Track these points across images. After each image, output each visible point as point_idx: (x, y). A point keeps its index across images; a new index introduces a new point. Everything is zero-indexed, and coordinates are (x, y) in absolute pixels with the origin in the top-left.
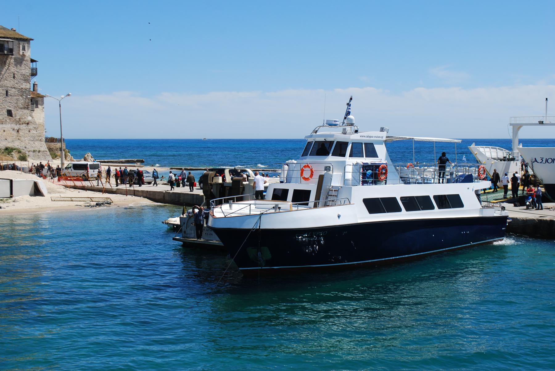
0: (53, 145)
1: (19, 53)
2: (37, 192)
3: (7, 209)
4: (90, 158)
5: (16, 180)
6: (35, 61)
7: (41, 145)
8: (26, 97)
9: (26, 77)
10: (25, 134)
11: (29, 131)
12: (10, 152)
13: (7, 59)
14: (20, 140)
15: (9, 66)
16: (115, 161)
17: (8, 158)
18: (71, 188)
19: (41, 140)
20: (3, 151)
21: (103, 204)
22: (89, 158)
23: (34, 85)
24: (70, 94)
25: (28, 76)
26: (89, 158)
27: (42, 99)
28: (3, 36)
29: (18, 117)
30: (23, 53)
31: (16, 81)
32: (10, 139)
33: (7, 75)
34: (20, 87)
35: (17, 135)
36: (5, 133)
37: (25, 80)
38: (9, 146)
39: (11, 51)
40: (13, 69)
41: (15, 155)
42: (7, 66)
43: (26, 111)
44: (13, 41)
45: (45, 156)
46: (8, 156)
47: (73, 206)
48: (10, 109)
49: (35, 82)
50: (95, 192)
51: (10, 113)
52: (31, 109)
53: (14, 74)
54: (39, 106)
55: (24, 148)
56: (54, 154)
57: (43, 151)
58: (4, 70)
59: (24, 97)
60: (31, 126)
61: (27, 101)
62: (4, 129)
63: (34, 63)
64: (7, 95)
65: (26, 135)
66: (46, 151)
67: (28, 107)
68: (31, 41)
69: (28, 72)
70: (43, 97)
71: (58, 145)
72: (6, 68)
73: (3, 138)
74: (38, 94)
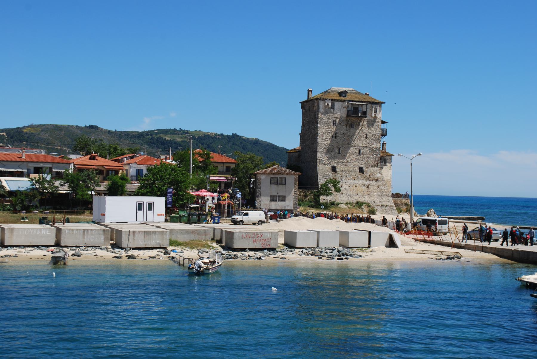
0: (398, 200)
1: (371, 115)
2: (392, 243)
3: (366, 258)
4: (433, 214)
5: (374, 232)
6: (386, 123)
7: (388, 201)
8: (377, 155)
9: (376, 137)
10: (374, 190)
11: (378, 187)
12: (361, 206)
13: (360, 121)
14: (370, 195)
15: (362, 127)
16: (456, 218)
17: (359, 211)
18: (421, 241)
19: (388, 196)
20: (354, 204)
21: (453, 258)
22: (432, 214)
23: (383, 144)
24: (421, 153)
25: (378, 136)
26: (432, 214)
27: (390, 157)
28: (358, 100)
30: (375, 115)
31: (368, 141)
32: (360, 194)
33: (360, 135)
34: (371, 147)
35: (367, 190)
36: (356, 188)
37: (376, 140)
38: (360, 200)
39: (365, 113)
40: (366, 130)
41: (365, 209)
42: (361, 128)
43: (376, 169)
44: (366, 105)
45: (391, 210)
46: (358, 209)
47: (425, 258)
48: (362, 166)
49: (384, 142)
50: (444, 247)
51: (361, 170)
52: (380, 167)
53: (366, 135)
54: (387, 163)
55: (373, 203)
56: (400, 209)
57: (390, 206)
58: (358, 131)
59: (375, 155)
60: (380, 183)
61: (377, 159)
62: (356, 185)
63: (385, 124)
64: (359, 153)
65: (375, 190)
66: (393, 206)
67: (378, 165)
68: (382, 104)
69: (378, 132)
70: (391, 155)
71: (404, 200)
72: (360, 129)
73: (355, 193)
74: (387, 152)
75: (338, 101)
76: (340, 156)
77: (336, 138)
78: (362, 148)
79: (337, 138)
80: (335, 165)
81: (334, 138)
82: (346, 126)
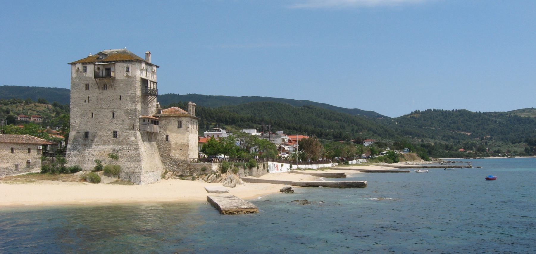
29: (122, 138)
48: (116, 130)
51: (115, 134)
59: (130, 118)
64: (113, 117)
75: (89, 63)
76: (93, 121)
77: (89, 102)
78: (115, 110)
79: (90, 102)
80: (88, 131)
81: (87, 102)
82: (99, 89)
